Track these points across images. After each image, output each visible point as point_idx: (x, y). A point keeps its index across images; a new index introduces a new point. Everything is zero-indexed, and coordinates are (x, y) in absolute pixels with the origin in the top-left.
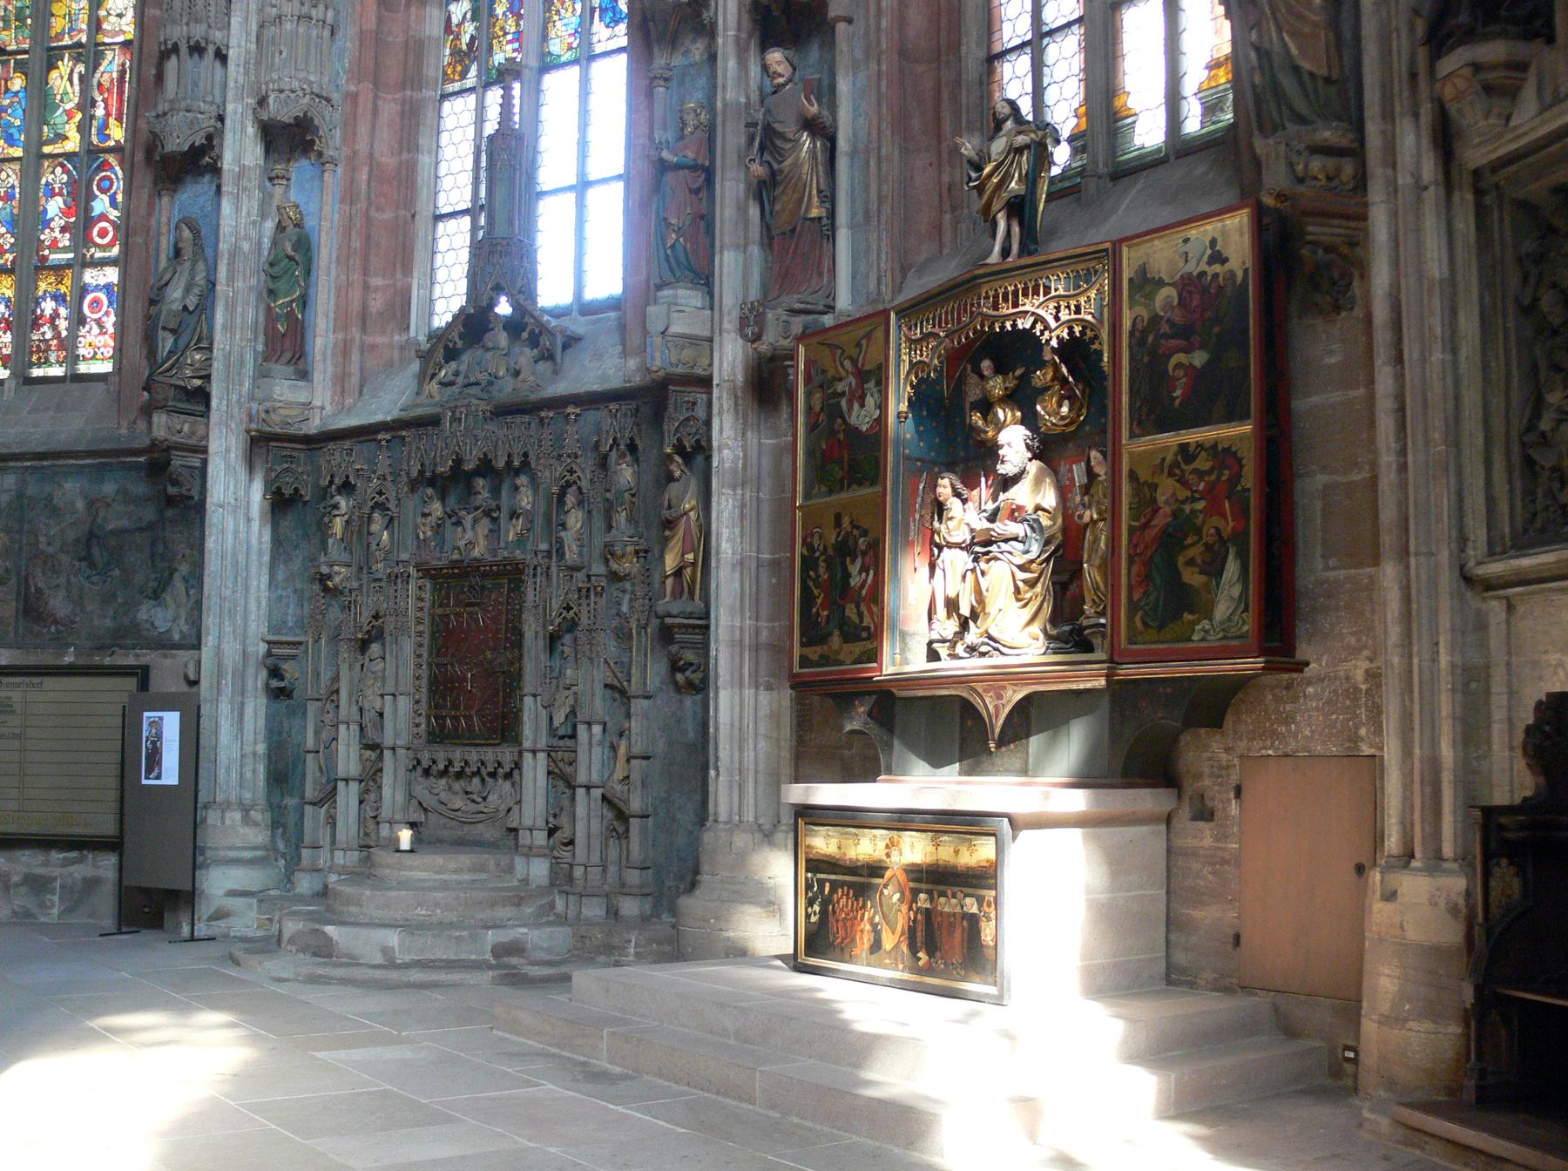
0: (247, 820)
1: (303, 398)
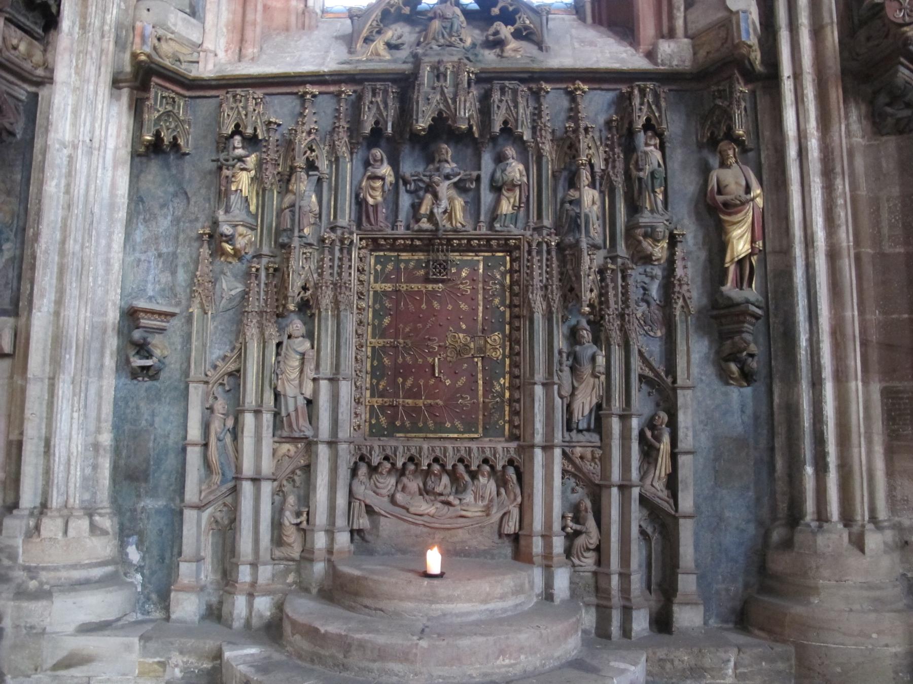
0: (94, 529)
1: (195, 37)
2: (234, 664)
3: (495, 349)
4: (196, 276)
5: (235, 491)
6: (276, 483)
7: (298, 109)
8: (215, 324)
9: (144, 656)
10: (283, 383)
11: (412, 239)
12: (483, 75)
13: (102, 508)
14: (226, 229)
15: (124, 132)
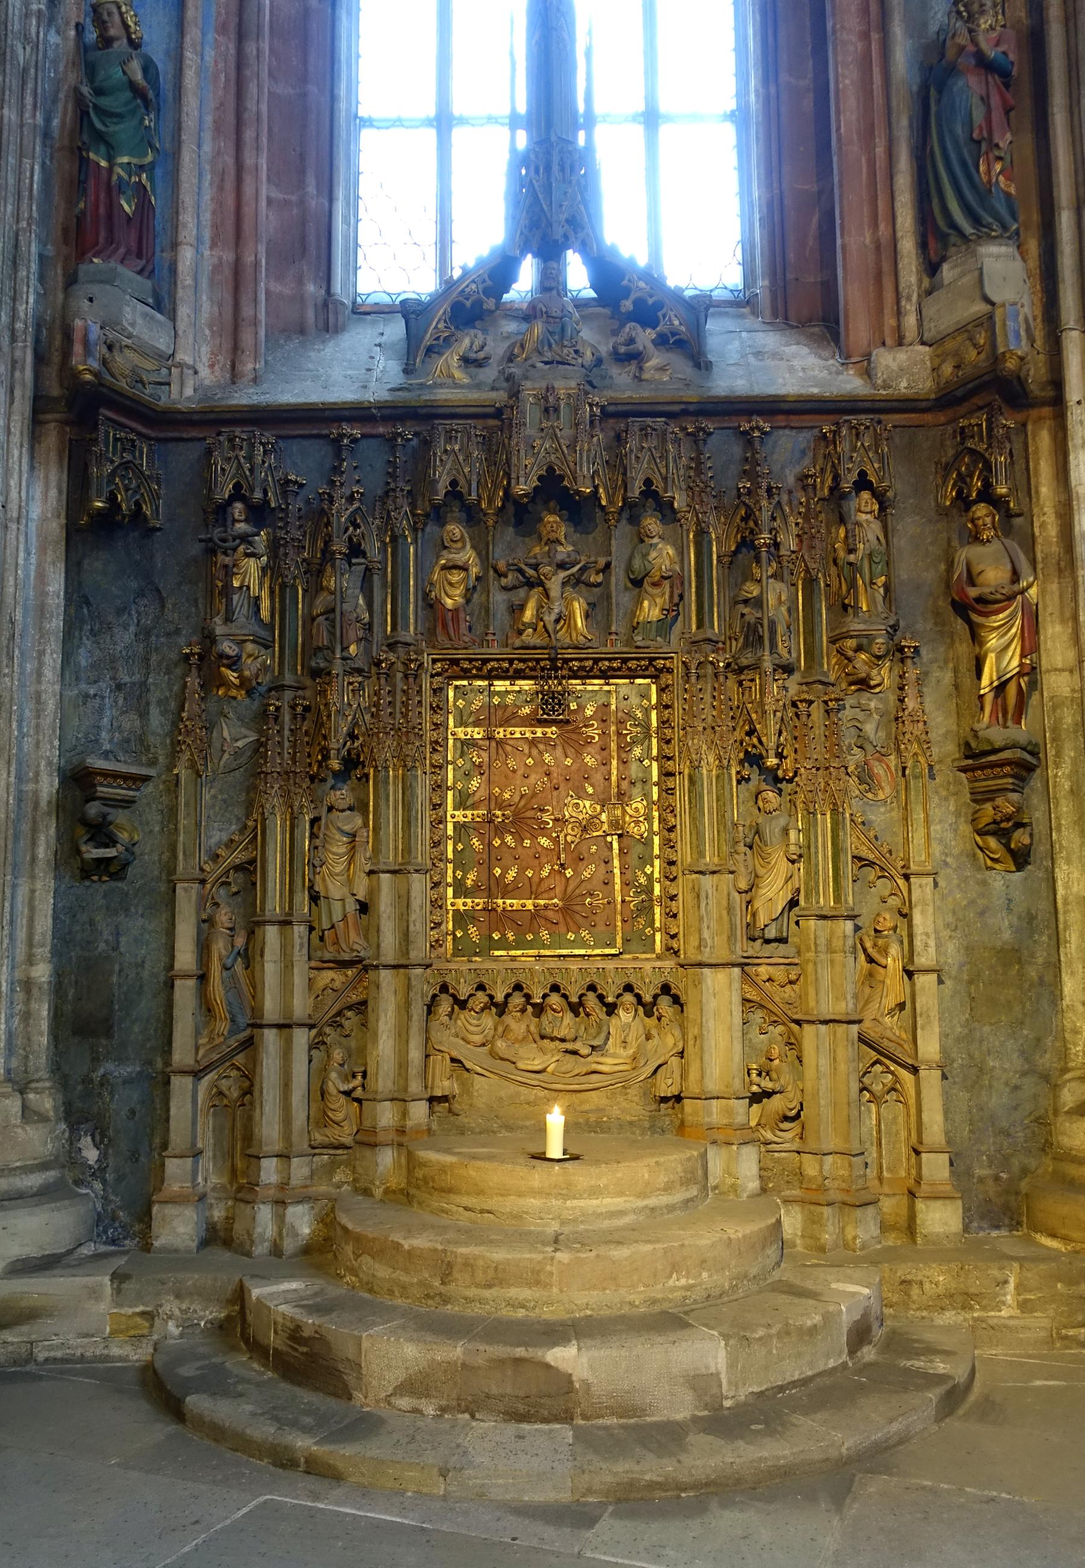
1: (162, 343)
2: (271, 1305)
3: (637, 823)
4: (182, 720)
5: (249, 1044)
6: (314, 1032)
7: (329, 463)
8: (213, 791)
9: (119, 1305)
10: (324, 880)
11: (511, 661)
12: (612, 409)
13: (37, 1081)
14: (227, 647)
15: (53, 493)
